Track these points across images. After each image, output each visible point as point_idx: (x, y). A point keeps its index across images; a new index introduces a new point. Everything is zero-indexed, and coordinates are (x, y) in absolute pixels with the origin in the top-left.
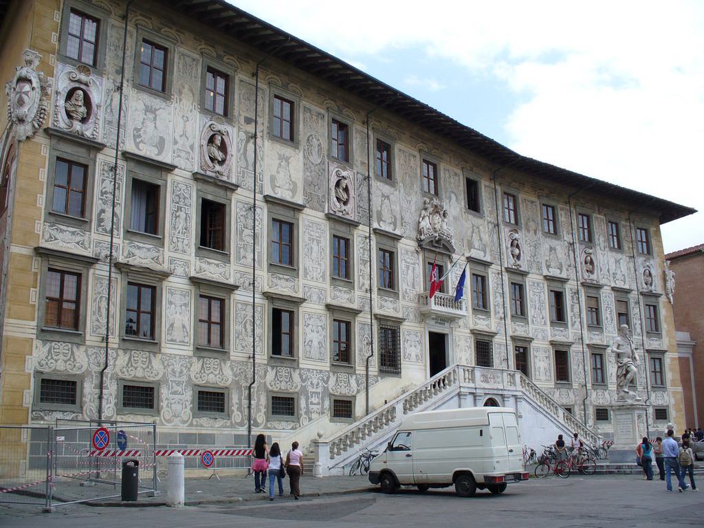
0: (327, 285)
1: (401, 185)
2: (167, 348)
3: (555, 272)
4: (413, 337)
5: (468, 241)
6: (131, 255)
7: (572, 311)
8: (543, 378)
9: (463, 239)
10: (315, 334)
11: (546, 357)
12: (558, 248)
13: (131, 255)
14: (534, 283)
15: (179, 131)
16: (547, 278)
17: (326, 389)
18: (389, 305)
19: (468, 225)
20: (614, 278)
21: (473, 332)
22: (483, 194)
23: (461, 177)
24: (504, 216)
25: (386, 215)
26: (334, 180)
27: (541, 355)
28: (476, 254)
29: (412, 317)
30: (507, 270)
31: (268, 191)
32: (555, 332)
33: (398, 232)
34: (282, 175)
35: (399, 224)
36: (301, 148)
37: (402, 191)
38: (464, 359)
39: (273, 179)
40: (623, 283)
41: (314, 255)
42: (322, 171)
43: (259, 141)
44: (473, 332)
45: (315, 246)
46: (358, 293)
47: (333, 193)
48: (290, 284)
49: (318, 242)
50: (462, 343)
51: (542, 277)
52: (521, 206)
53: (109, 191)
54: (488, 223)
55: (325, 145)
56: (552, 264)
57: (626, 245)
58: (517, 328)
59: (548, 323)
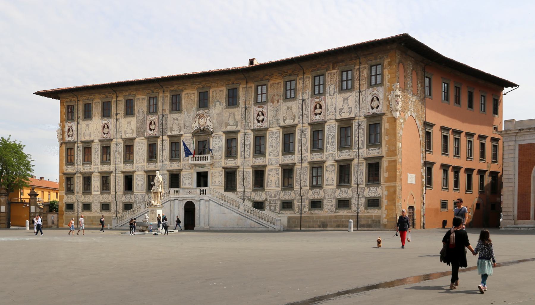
0: (145, 164)
1: (185, 110)
2: (93, 193)
3: (289, 122)
4: (187, 176)
5: (226, 123)
6: (84, 169)
7: (299, 143)
8: (273, 185)
9: (222, 124)
10: (140, 182)
11: (277, 174)
12: (294, 106)
13: (84, 169)
14: (273, 133)
15: (95, 128)
16: (282, 127)
17: (144, 201)
18: (175, 165)
19: (228, 114)
20: (339, 113)
21: (223, 168)
22: (240, 93)
23: (225, 91)
24: (256, 98)
25: (175, 127)
26: (148, 123)
27: (274, 173)
28: (229, 129)
29: (187, 167)
30: (252, 130)
31: (124, 137)
32: (285, 159)
33: (182, 133)
34: (128, 129)
35: (182, 128)
36: (135, 116)
37: (186, 113)
38: (217, 182)
39: (125, 131)
40: (348, 113)
41: (140, 154)
42: (144, 121)
43: (120, 120)
44: (223, 168)
45: (140, 151)
46: (159, 163)
47: (148, 128)
48: (131, 166)
49: (142, 149)
50: (217, 174)
51: (279, 128)
52: (269, 89)
53: (79, 154)
54: (242, 108)
55: (145, 110)
56: (288, 118)
57: (357, 85)
58: (256, 161)
59: (281, 154)
